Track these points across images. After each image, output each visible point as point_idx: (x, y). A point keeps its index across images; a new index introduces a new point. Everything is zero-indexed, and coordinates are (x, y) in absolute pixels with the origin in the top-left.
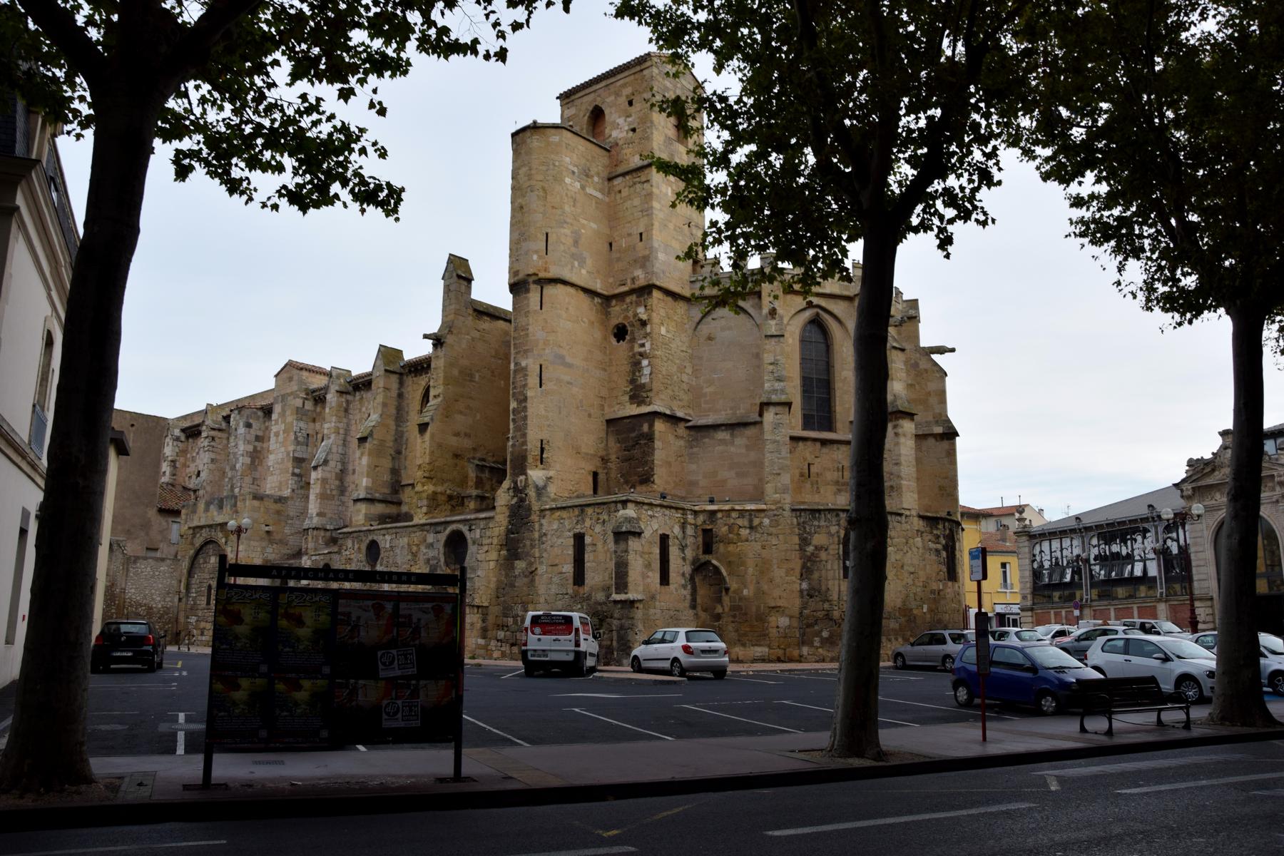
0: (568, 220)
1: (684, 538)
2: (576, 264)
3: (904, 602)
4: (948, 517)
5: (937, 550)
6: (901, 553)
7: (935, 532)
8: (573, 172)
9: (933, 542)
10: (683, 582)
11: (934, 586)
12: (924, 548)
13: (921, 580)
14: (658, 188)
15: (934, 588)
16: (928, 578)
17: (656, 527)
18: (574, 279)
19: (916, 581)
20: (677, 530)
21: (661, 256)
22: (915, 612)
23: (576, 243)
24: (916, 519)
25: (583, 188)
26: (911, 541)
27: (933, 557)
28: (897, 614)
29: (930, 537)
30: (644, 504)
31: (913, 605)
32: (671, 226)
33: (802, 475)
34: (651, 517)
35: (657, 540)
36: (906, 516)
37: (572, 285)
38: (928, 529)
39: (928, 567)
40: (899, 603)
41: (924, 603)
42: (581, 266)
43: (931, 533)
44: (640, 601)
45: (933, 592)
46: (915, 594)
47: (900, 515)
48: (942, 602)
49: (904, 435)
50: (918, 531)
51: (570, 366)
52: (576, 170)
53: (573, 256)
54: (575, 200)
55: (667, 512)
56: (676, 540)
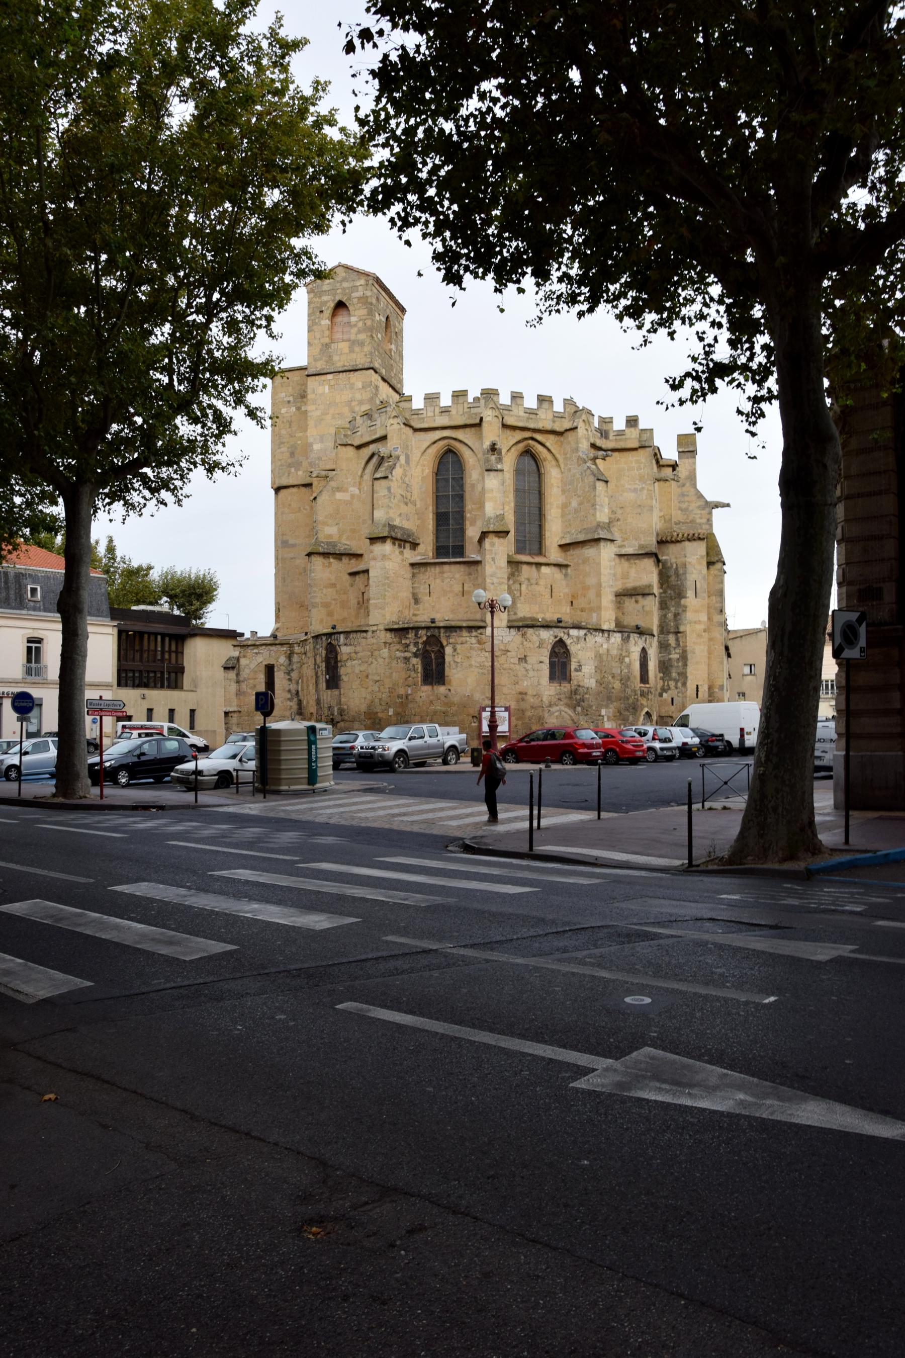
0: (284, 440)
1: (290, 664)
2: (293, 470)
3: (369, 707)
4: (433, 625)
5: (407, 659)
6: (366, 665)
7: (403, 642)
8: (289, 402)
9: (401, 651)
10: (289, 696)
11: (402, 691)
12: (390, 657)
13: (387, 686)
14: (314, 392)
15: (401, 693)
16: (394, 684)
17: (260, 659)
18: (291, 482)
19: (382, 688)
20: (282, 660)
21: (317, 447)
22: (380, 715)
23: (292, 454)
24: (383, 633)
25: (298, 409)
26: (376, 653)
27: (401, 665)
28: (362, 717)
29: (398, 647)
30: (249, 646)
31: (378, 709)
32: (329, 417)
33: (359, 603)
34: (256, 653)
35: (263, 669)
36: (373, 632)
37: (293, 486)
38: (397, 639)
39: (394, 674)
40: (363, 708)
41: (390, 707)
42: (297, 470)
43: (400, 643)
44: (234, 712)
45: (399, 696)
46: (380, 699)
47: (366, 631)
48: (411, 706)
49: (374, 559)
50: (385, 643)
51: (293, 546)
52: (291, 399)
53: (290, 466)
54: (290, 423)
55: (273, 648)
56: (282, 668)
